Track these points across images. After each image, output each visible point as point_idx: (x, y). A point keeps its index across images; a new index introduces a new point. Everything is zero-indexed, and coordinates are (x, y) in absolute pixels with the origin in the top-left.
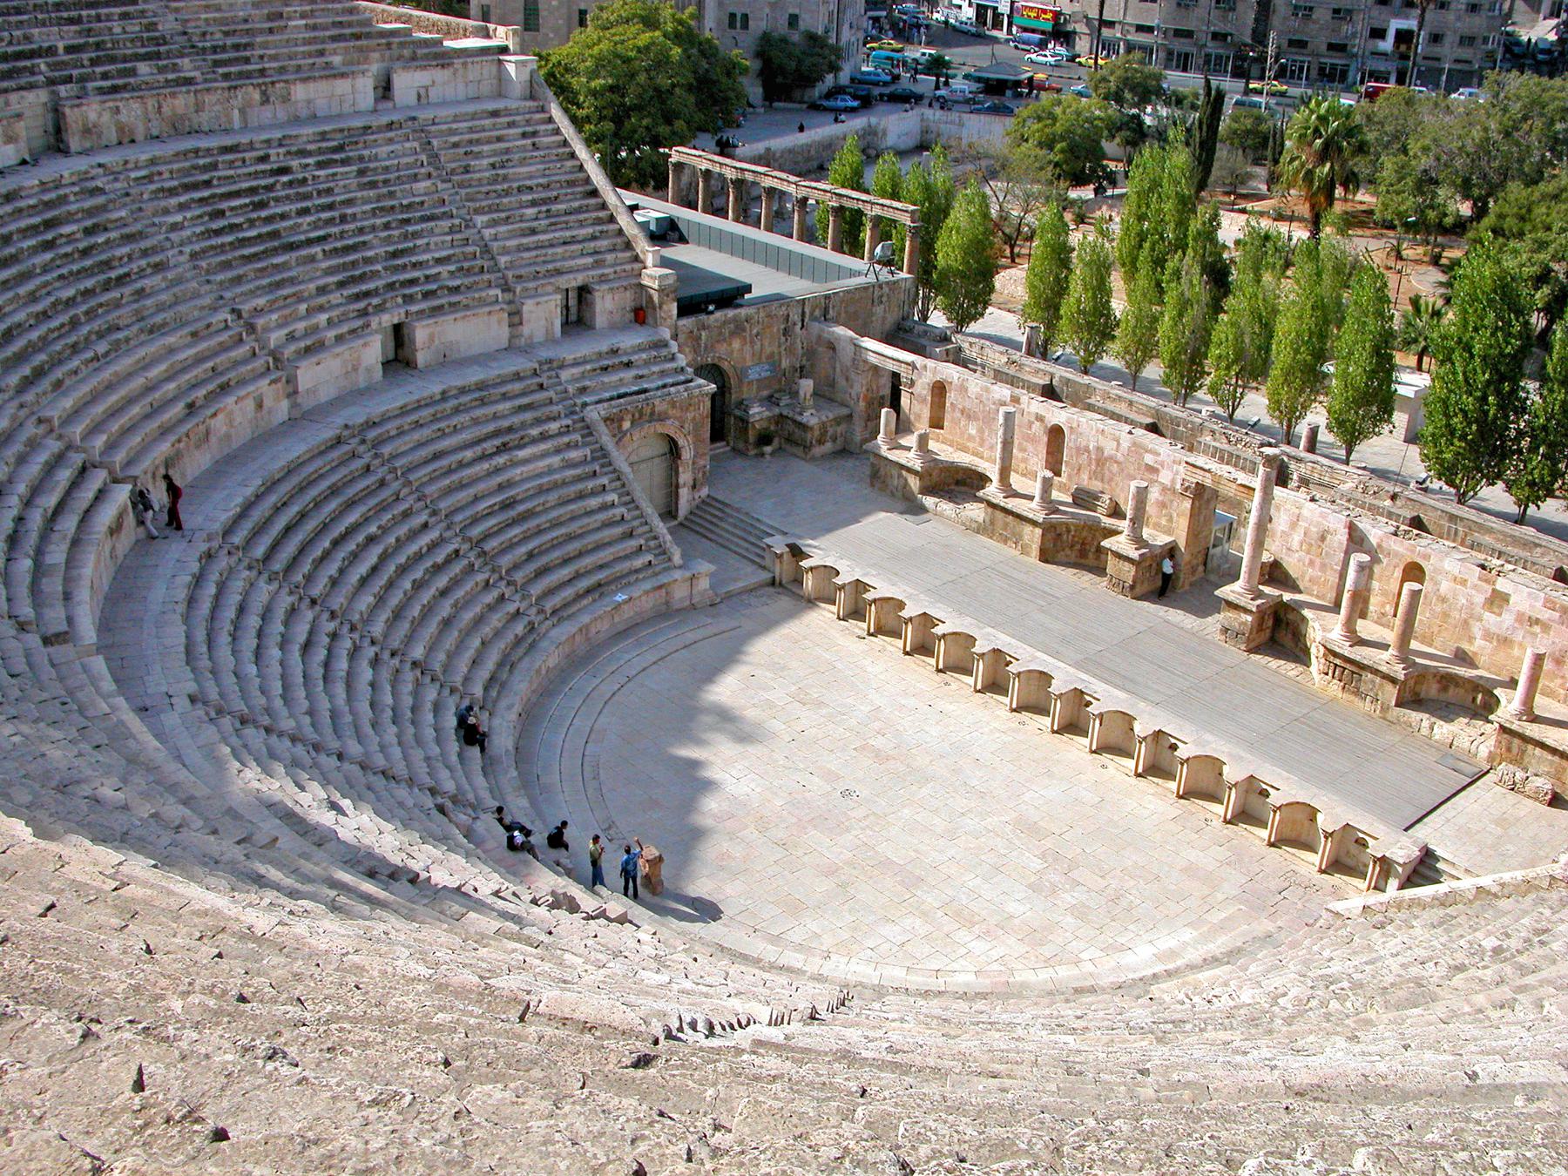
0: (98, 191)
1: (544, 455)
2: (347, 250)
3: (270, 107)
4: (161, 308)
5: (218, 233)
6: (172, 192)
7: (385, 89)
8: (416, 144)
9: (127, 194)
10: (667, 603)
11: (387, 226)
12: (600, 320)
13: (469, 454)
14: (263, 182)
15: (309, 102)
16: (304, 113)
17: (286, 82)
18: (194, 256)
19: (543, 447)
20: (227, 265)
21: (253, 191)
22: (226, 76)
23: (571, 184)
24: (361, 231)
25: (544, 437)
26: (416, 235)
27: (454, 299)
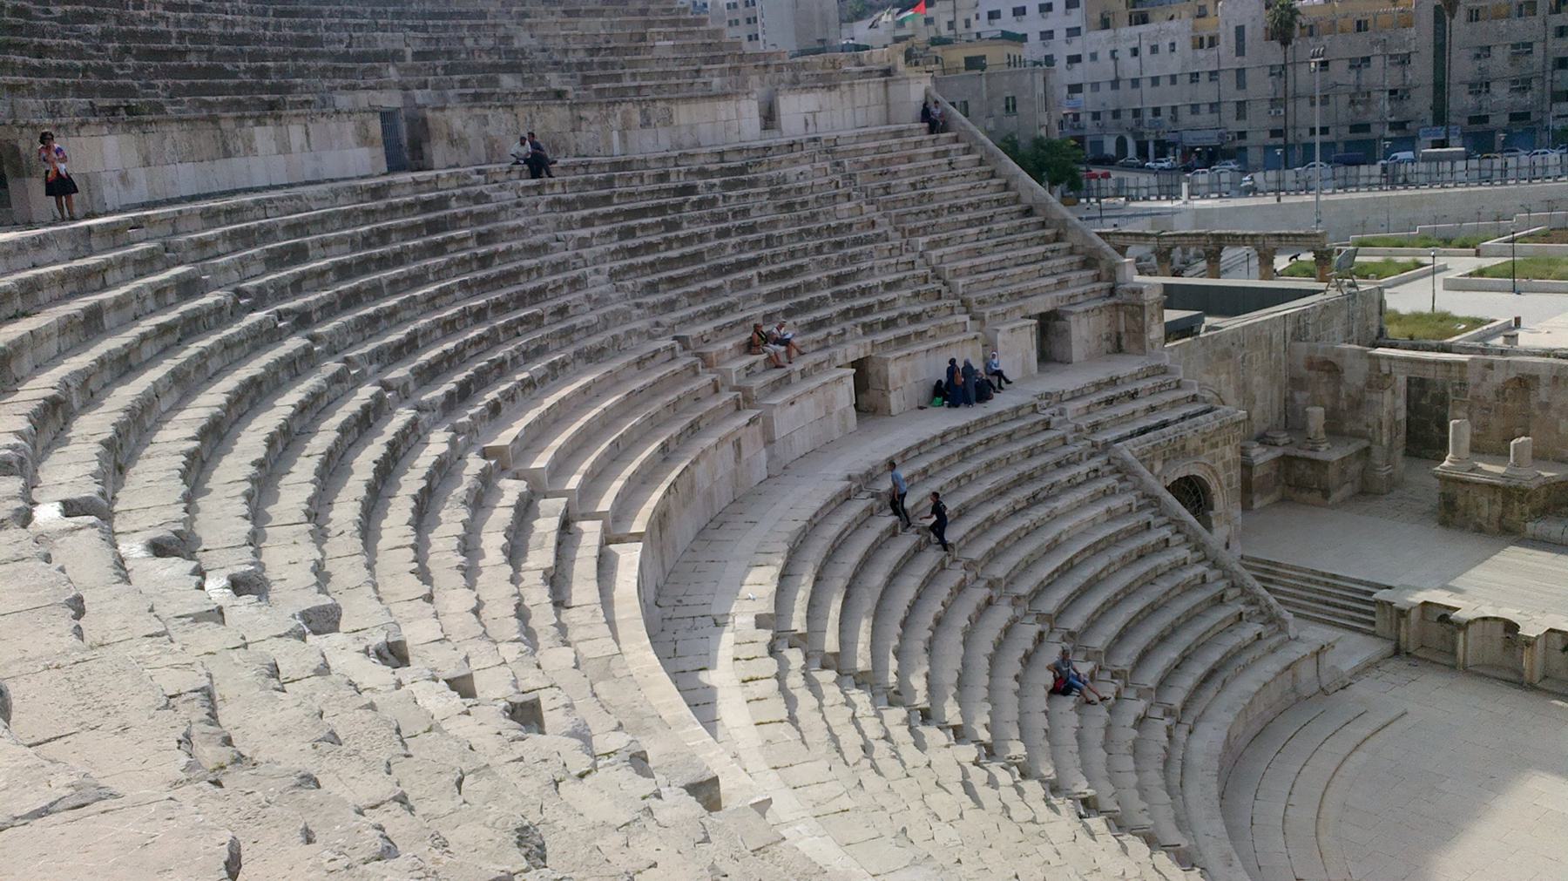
0: (481, 198)
1: (1081, 506)
2: (785, 274)
3: (648, 131)
4: (589, 330)
5: (633, 252)
6: (570, 205)
7: (769, 117)
8: (827, 165)
9: (519, 205)
10: (1294, 689)
11: (819, 249)
12: (1077, 352)
13: (1001, 506)
14: (672, 200)
15: (692, 127)
16: (687, 141)
17: (667, 100)
18: (613, 275)
19: (1083, 493)
20: (652, 288)
21: (660, 210)
22: (600, 92)
23: (1000, 202)
24: (792, 254)
25: (1073, 485)
26: (854, 258)
27: (920, 327)
